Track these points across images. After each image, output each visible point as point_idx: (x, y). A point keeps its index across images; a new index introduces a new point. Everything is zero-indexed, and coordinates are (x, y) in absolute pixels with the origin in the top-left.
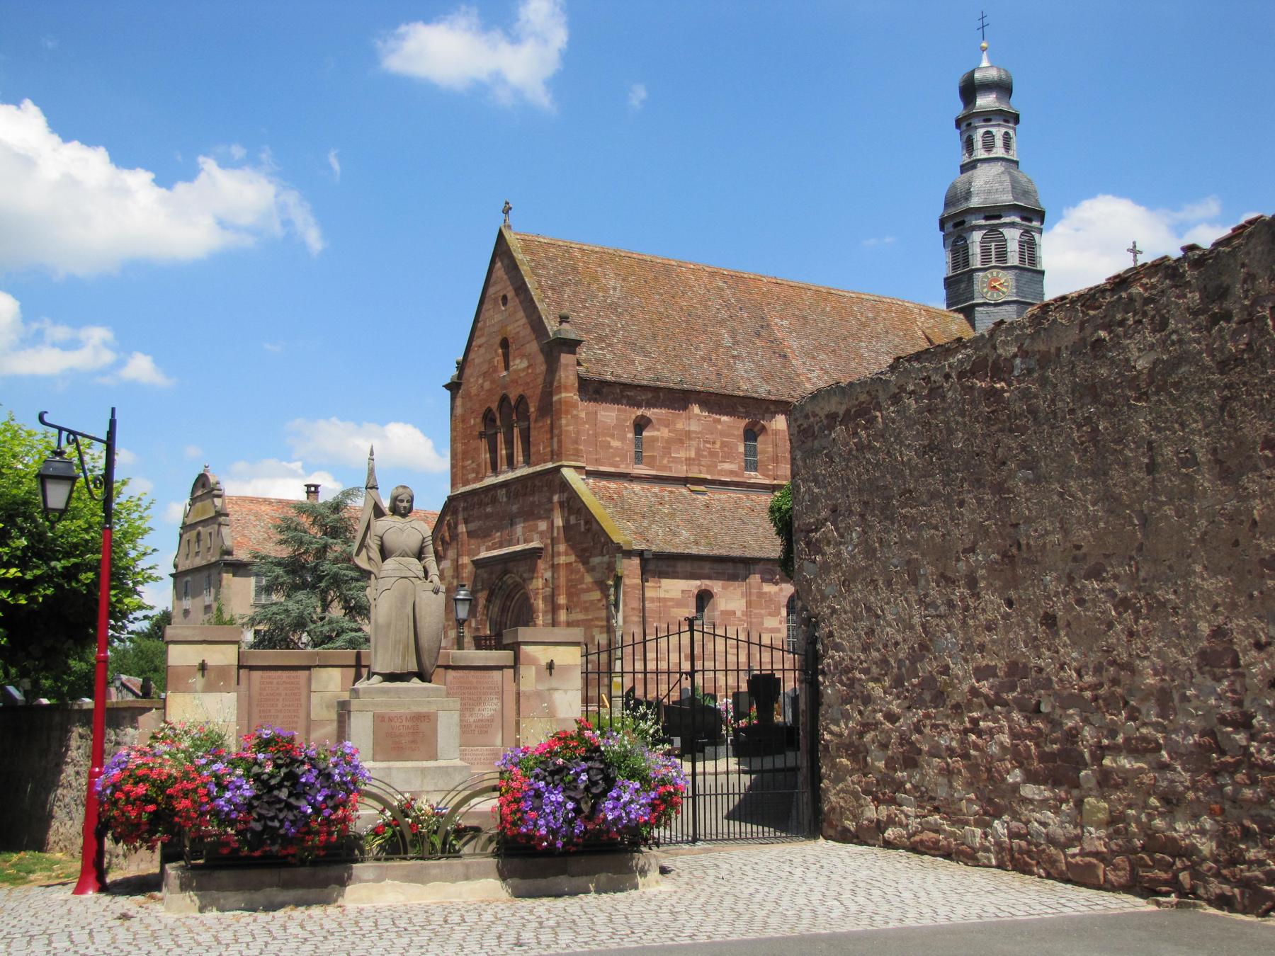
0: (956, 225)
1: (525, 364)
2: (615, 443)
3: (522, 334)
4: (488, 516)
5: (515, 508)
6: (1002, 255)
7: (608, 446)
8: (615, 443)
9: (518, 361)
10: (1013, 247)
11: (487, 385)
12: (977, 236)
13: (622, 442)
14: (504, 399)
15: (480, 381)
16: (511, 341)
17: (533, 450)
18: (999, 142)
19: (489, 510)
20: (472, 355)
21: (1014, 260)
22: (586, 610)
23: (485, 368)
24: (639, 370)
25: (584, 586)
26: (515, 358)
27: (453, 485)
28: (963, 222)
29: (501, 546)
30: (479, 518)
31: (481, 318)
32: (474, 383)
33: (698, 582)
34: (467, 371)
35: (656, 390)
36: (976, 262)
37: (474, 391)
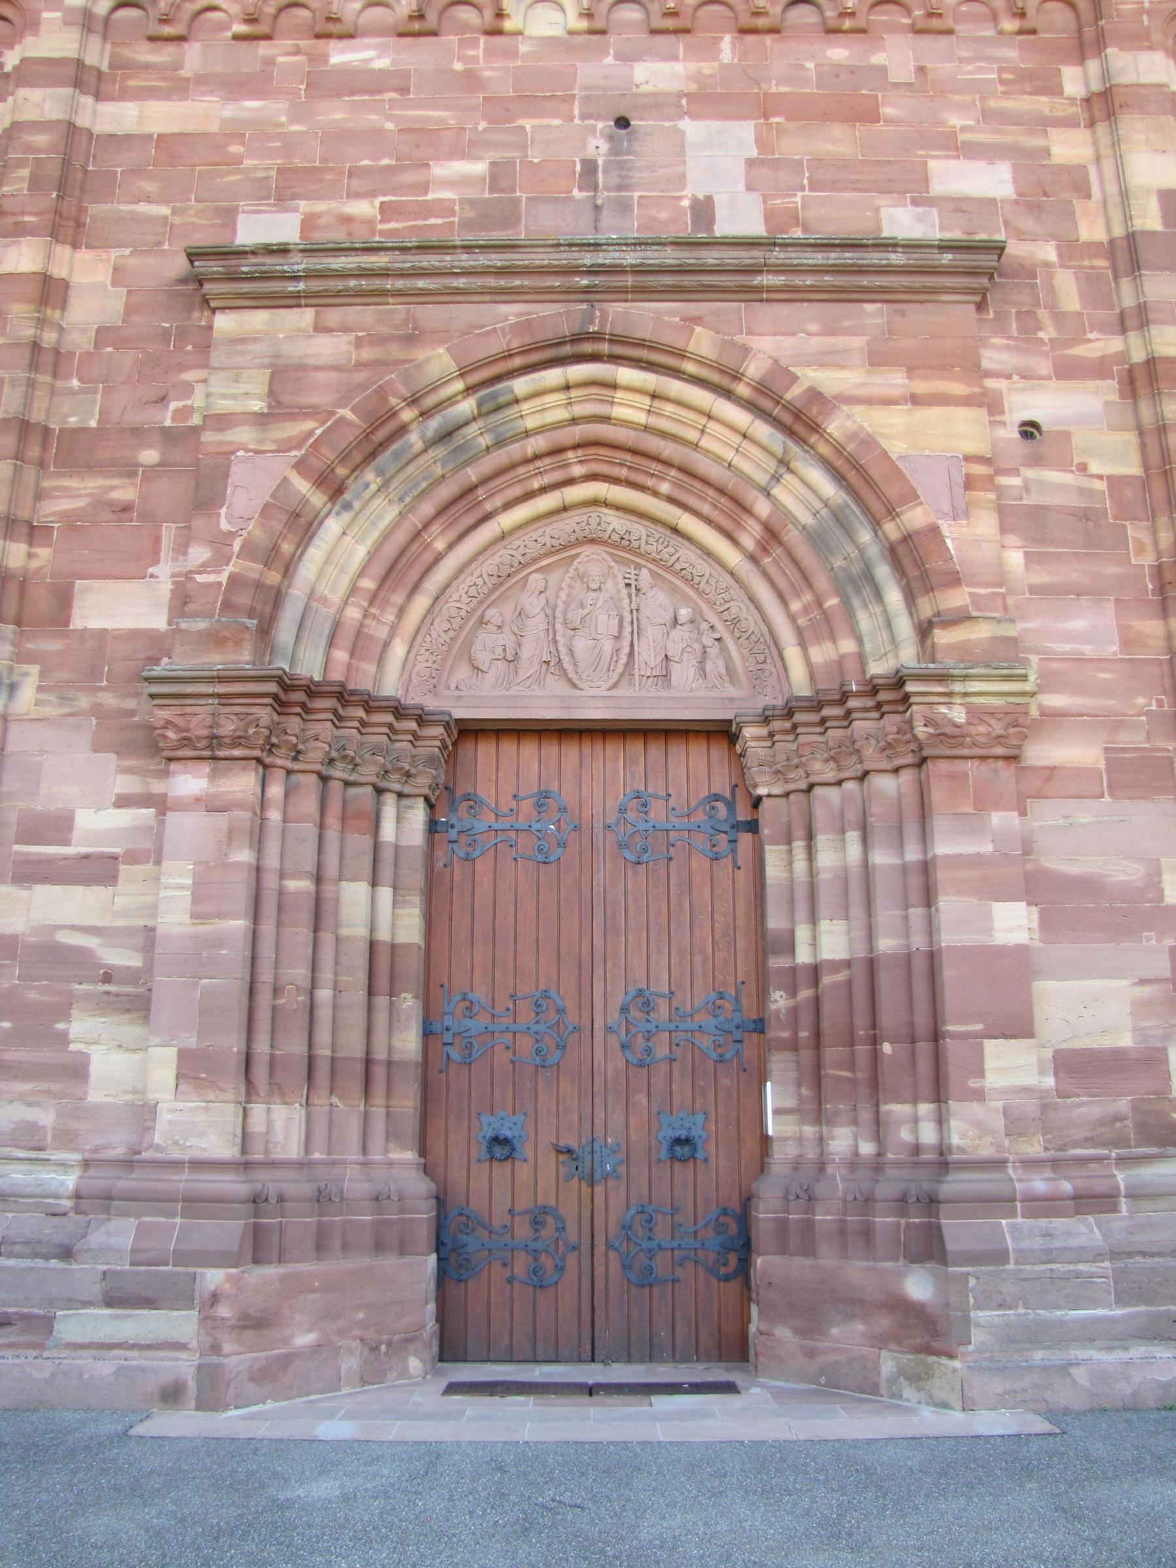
4: (325, 85)
5: (660, 74)
30: (236, 87)
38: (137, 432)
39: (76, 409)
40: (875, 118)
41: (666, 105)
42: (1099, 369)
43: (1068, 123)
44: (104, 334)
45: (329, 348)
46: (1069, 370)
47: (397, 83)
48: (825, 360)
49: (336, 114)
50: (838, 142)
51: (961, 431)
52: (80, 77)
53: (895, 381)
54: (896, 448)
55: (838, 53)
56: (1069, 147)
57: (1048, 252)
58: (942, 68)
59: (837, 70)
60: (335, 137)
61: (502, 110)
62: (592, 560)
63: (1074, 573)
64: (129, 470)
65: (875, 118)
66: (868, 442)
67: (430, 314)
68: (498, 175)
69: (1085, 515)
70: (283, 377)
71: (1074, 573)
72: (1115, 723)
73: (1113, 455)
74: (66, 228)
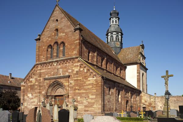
0: (111, 34)
1: (64, 34)
2: (86, 55)
3: (63, 28)
4: (48, 69)
5: (59, 67)
6: (118, 40)
7: (85, 55)
8: (86, 55)
9: (61, 34)
10: (120, 39)
11: (50, 39)
12: (115, 36)
13: (86, 55)
14: (56, 43)
15: (47, 39)
16: (59, 29)
17: (66, 54)
18: (117, 22)
19: (49, 67)
20: (44, 33)
21: (120, 41)
22: (86, 90)
23: (49, 35)
24: (88, 40)
25: (86, 85)
26: (60, 33)
27: (36, 62)
28: (113, 33)
29: (54, 75)
30: (45, 69)
31: (48, 24)
32: (44, 38)
33: (109, 86)
34: (42, 37)
35: (92, 45)
36: (114, 40)
37: (45, 41)
38: (43, 86)
39: (41, 85)
40: (66, 68)
41: (59, 68)
42: (73, 80)
43: (74, 67)
44: (42, 81)
45: (48, 82)
46: (72, 80)
47: (50, 68)
48: (63, 81)
49: (48, 70)
50: (65, 70)
51: (67, 84)
52: (40, 70)
53: (65, 82)
54: (65, 85)
55: (65, 65)
56: (74, 68)
57: (72, 74)
58: (69, 65)
59: (65, 66)
60: (48, 71)
61: (54, 69)
62: (60, 88)
63: (71, 89)
64: (43, 87)
65: (66, 68)
66: (64, 84)
67: (51, 80)
68: (54, 72)
69: (72, 87)
70: (47, 83)
71: (71, 89)
72: (72, 95)
73: (73, 84)
74: (40, 77)
